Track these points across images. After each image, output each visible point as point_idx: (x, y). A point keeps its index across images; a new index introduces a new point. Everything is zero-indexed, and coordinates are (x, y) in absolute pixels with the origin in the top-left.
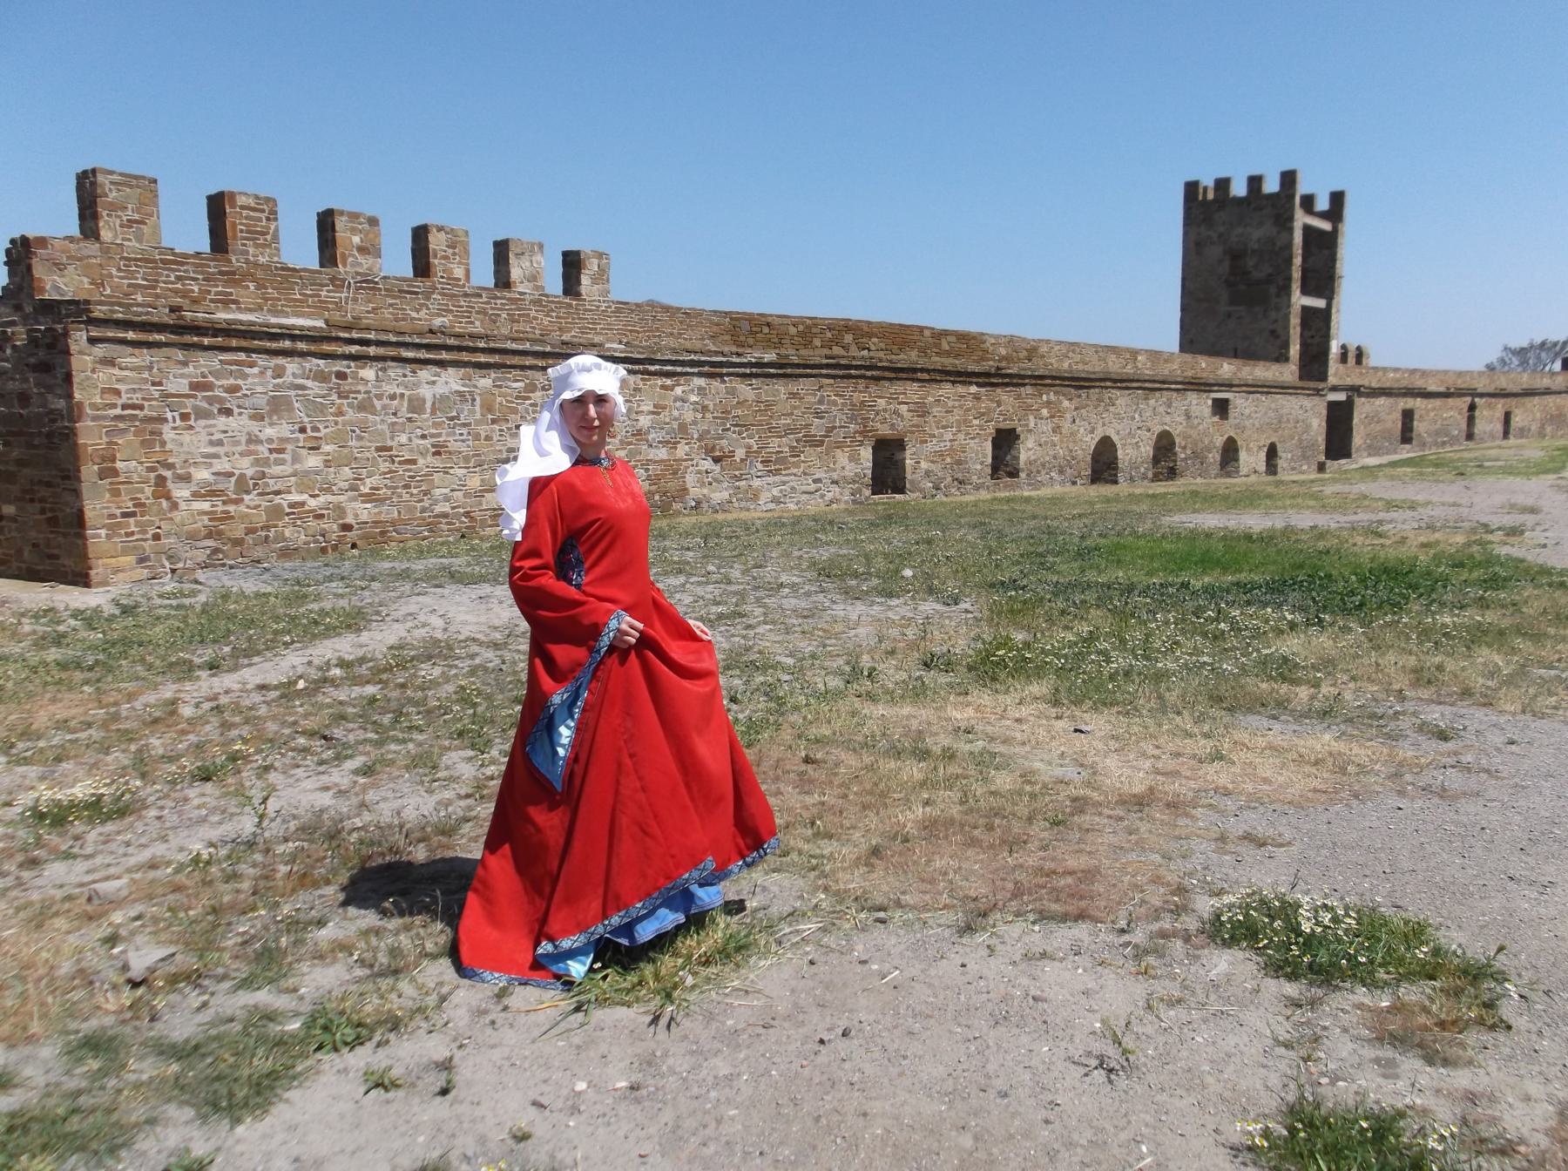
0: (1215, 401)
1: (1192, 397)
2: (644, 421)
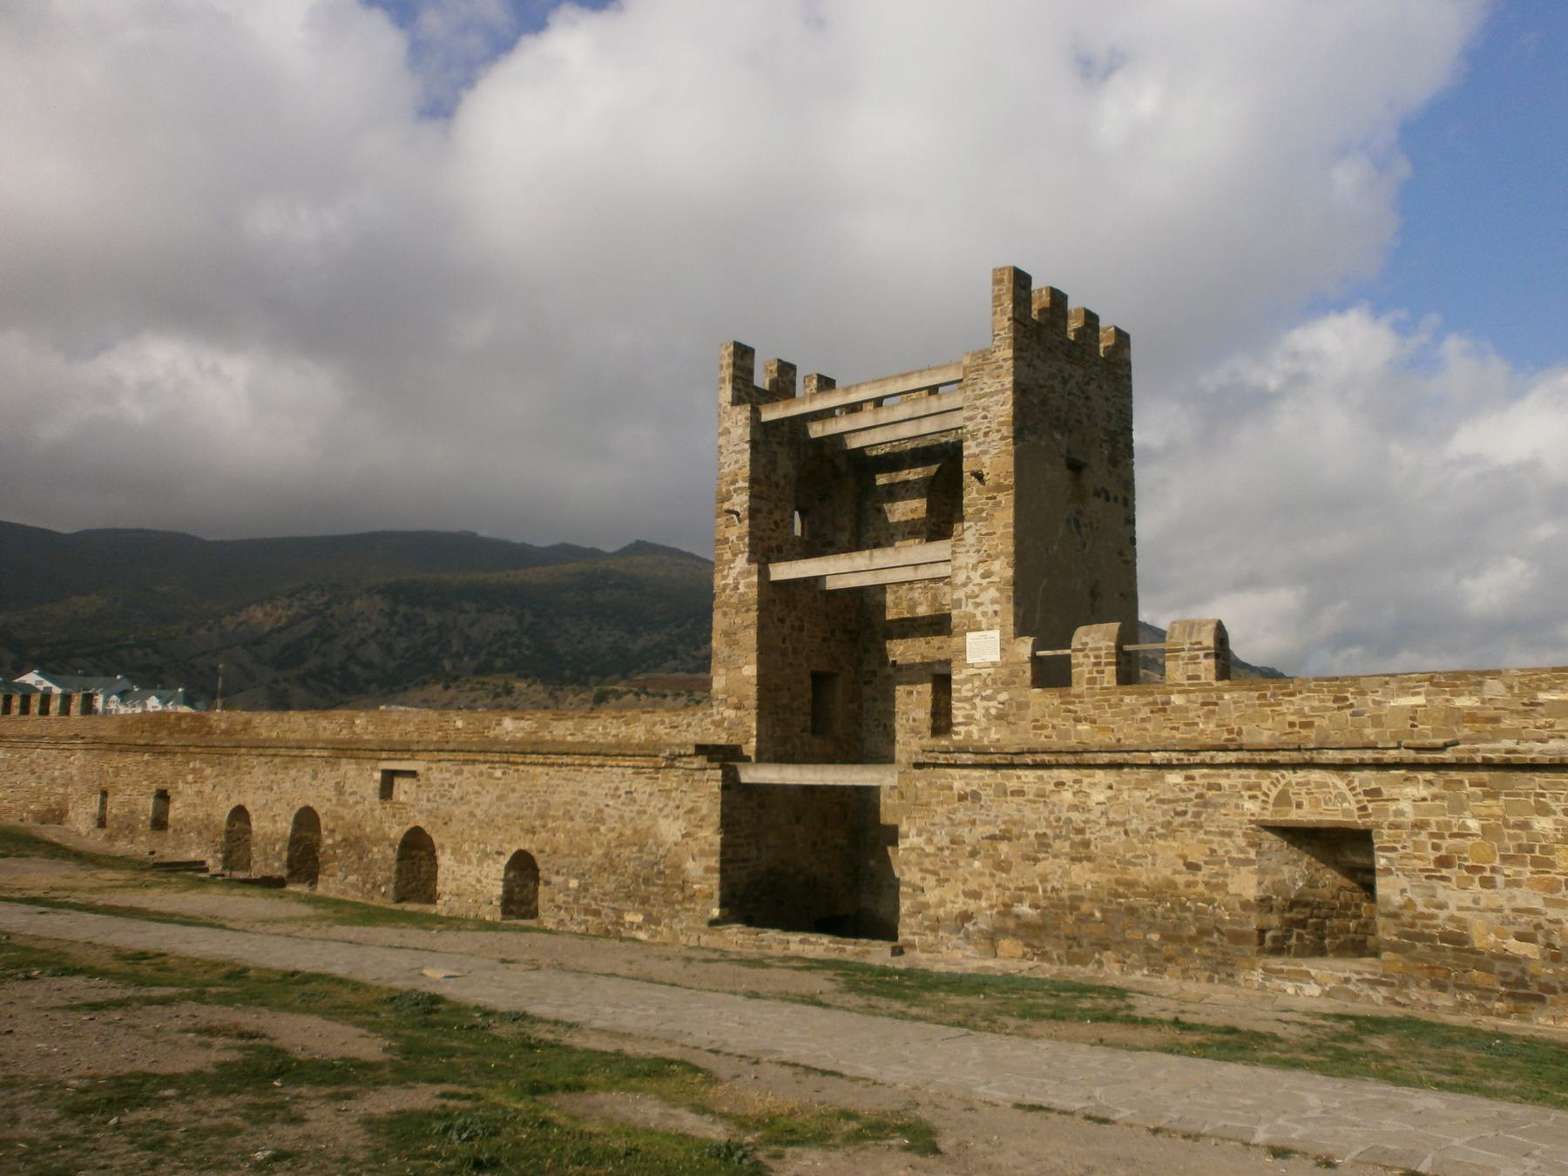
1: (348, 768)
2: (57, 773)
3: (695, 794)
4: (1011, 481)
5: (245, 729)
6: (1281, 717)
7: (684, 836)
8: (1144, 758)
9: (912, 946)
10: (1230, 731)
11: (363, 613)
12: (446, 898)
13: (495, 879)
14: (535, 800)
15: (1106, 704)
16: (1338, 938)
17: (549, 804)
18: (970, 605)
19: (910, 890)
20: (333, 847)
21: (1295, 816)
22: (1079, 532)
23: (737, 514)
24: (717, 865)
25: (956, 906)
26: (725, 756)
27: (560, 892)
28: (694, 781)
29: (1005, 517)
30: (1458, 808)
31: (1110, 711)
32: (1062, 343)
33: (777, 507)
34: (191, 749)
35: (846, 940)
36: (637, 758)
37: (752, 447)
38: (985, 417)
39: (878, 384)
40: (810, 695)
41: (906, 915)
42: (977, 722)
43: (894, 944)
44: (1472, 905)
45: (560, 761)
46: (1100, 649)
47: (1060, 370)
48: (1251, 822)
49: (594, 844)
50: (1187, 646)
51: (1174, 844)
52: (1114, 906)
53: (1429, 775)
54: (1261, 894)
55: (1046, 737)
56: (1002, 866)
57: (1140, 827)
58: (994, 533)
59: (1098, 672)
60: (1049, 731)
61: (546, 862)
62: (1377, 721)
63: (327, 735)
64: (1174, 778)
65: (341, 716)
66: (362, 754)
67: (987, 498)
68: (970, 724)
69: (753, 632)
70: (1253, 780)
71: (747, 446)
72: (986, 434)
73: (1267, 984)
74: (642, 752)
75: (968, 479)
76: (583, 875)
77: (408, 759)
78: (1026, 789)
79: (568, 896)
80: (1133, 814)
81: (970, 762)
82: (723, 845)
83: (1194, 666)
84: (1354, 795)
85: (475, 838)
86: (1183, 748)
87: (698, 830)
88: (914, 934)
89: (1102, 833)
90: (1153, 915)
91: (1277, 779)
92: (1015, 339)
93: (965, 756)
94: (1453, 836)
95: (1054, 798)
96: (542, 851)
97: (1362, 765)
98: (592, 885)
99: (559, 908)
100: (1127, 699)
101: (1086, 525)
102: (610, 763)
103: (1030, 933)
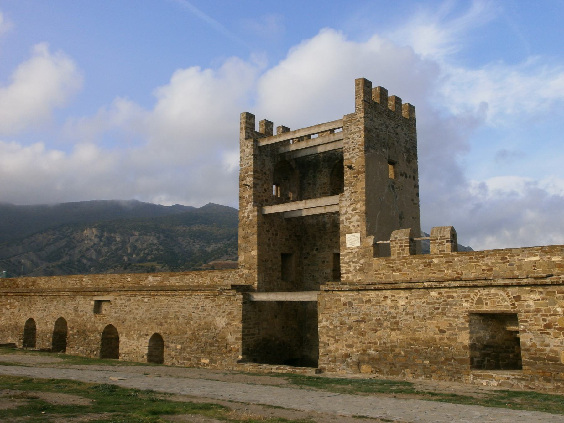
0: (96, 301)
1: (80, 300)
3: (231, 306)
4: (363, 169)
5: (33, 285)
6: (479, 267)
7: (226, 325)
8: (420, 285)
9: (324, 369)
10: (458, 274)
12: (123, 355)
13: (145, 346)
14: (162, 311)
15: (406, 263)
16: (505, 361)
17: (169, 313)
18: (347, 222)
19: (323, 345)
20: (73, 335)
21: (484, 308)
22: (394, 191)
23: (249, 186)
24: (241, 337)
25: (343, 351)
27: (173, 351)
28: (230, 300)
29: (361, 185)
30: (554, 303)
31: (407, 266)
32: (385, 111)
33: (265, 182)
34: (9, 294)
35: (297, 367)
36: (206, 291)
37: (254, 157)
38: (353, 142)
39: (307, 129)
40: (281, 263)
41: (321, 356)
42: (351, 272)
43: (317, 368)
44: (560, 345)
45: (173, 294)
46: (402, 240)
47: (385, 122)
48: (466, 311)
49: (188, 329)
50: (439, 238)
51: (434, 322)
52: (410, 349)
53: (541, 289)
54: (471, 342)
55: (380, 278)
56: (362, 333)
57: (419, 315)
58: (357, 192)
59: (402, 250)
60: (381, 276)
61: (167, 338)
62: (519, 268)
63: (71, 286)
64: (434, 294)
65: (77, 277)
66: (86, 293)
67: (354, 177)
68: (348, 273)
69: (256, 236)
70: (467, 293)
71: (252, 157)
72: (353, 150)
73: (475, 381)
74: (208, 289)
75: (346, 169)
76: (183, 343)
77: (106, 295)
78: (371, 300)
79: (177, 352)
80: (417, 309)
81: (348, 289)
82: (243, 328)
83: (442, 246)
84: (509, 299)
85: (136, 329)
86: (437, 280)
87: (233, 322)
88: (325, 364)
89: (404, 318)
90: (426, 353)
91: (477, 293)
92: (365, 109)
93: (345, 286)
94: (551, 315)
95: (384, 304)
96: (165, 333)
97: (512, 286)
98: (187, 347)
99: (173, 358)
100: (414, 261)
101: (397, 188)
102: (194, 294)
103: (374, 361)
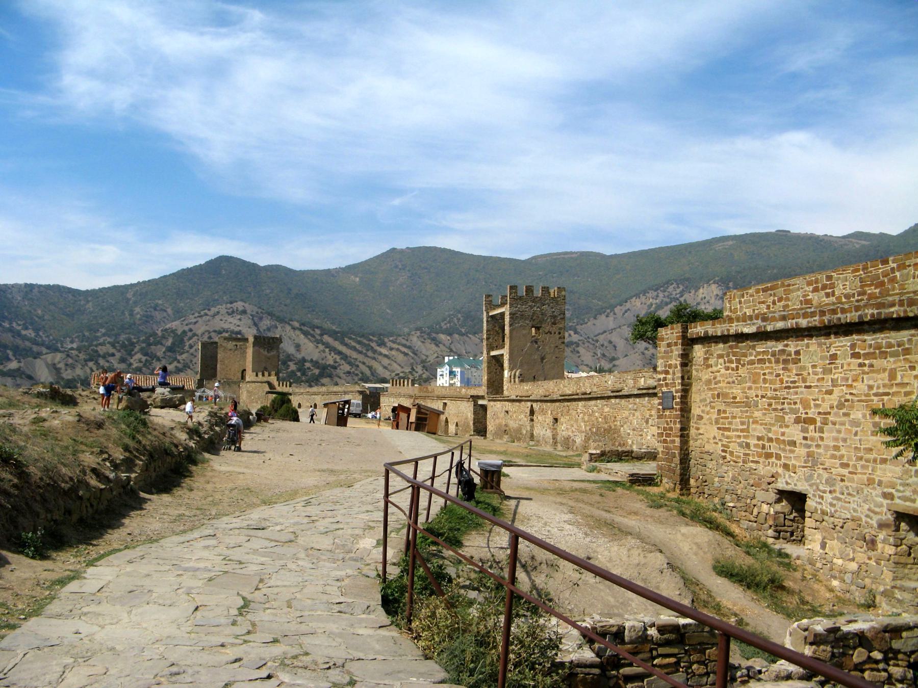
1: (439, 401)
11: (705, 298)
26: (475, 398)
